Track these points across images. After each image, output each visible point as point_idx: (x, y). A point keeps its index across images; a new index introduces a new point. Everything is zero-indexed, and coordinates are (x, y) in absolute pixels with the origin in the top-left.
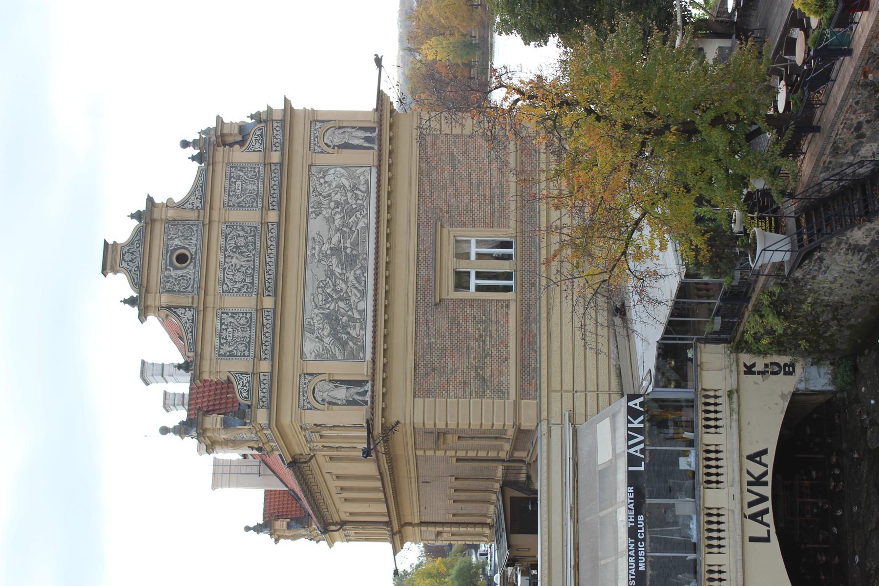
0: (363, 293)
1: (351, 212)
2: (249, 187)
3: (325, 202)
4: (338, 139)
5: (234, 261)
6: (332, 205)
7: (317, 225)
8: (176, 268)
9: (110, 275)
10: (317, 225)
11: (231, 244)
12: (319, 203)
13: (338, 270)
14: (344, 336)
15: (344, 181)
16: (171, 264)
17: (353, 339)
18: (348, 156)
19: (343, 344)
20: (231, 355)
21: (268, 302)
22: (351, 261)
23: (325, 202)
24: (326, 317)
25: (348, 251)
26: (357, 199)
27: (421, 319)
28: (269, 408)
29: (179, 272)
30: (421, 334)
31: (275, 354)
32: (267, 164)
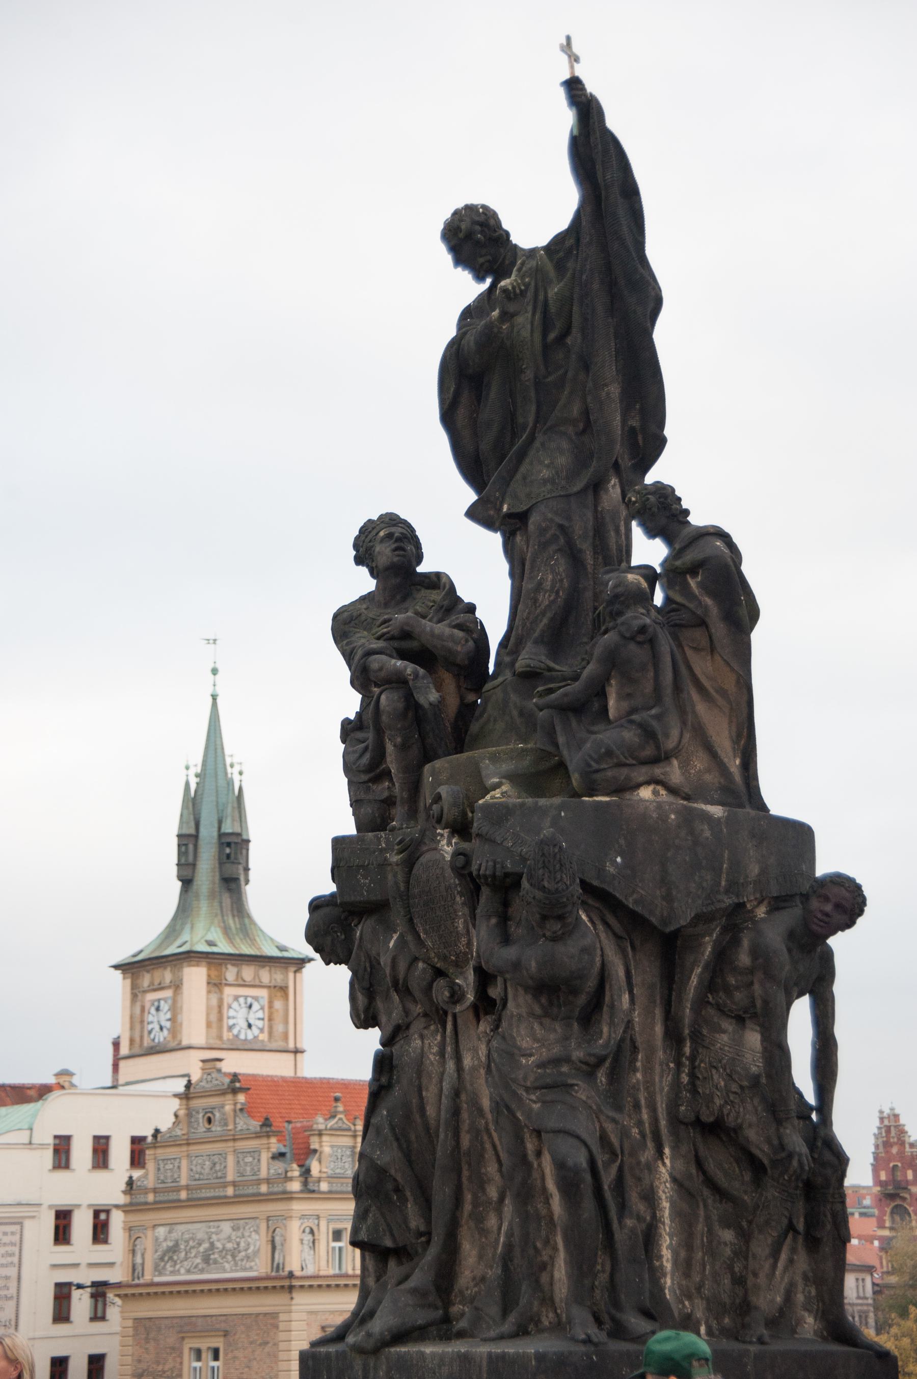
0: (188, 1271)
1: (234, 1257)
2: (248, 1169)
3: (239, 1234)
4: (278, 1239)
5: (207, 1163)
6: (238, 1240)
7: (226, 1227)
8: (204, 1116)
9: (201, 1064)
10: (226, 1227)
11: (216, 1159)
12: (238, 1229)
13: (201, 1249)
14: (166, 1258)
15: (252, 1248)
16: (206, 1113)
17: (165, 1265)
18: (266, 1249)
19: (162, 1259)
20: (159, 1169)
21: (183, 1195)
22: (206, 1260)
23: (239, 1234)
24: (177, 1245)
25: (212, 1257)
26: (242, 1260)
27: (175, 1321)
28: (131, 1204)
29: (201, 1121)
30: (167, 1322)
31: (157, 1206)
32: (259, 1182)
